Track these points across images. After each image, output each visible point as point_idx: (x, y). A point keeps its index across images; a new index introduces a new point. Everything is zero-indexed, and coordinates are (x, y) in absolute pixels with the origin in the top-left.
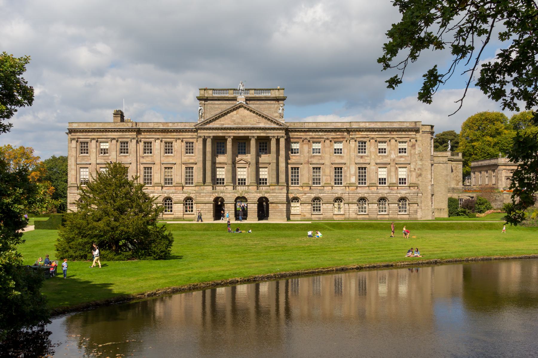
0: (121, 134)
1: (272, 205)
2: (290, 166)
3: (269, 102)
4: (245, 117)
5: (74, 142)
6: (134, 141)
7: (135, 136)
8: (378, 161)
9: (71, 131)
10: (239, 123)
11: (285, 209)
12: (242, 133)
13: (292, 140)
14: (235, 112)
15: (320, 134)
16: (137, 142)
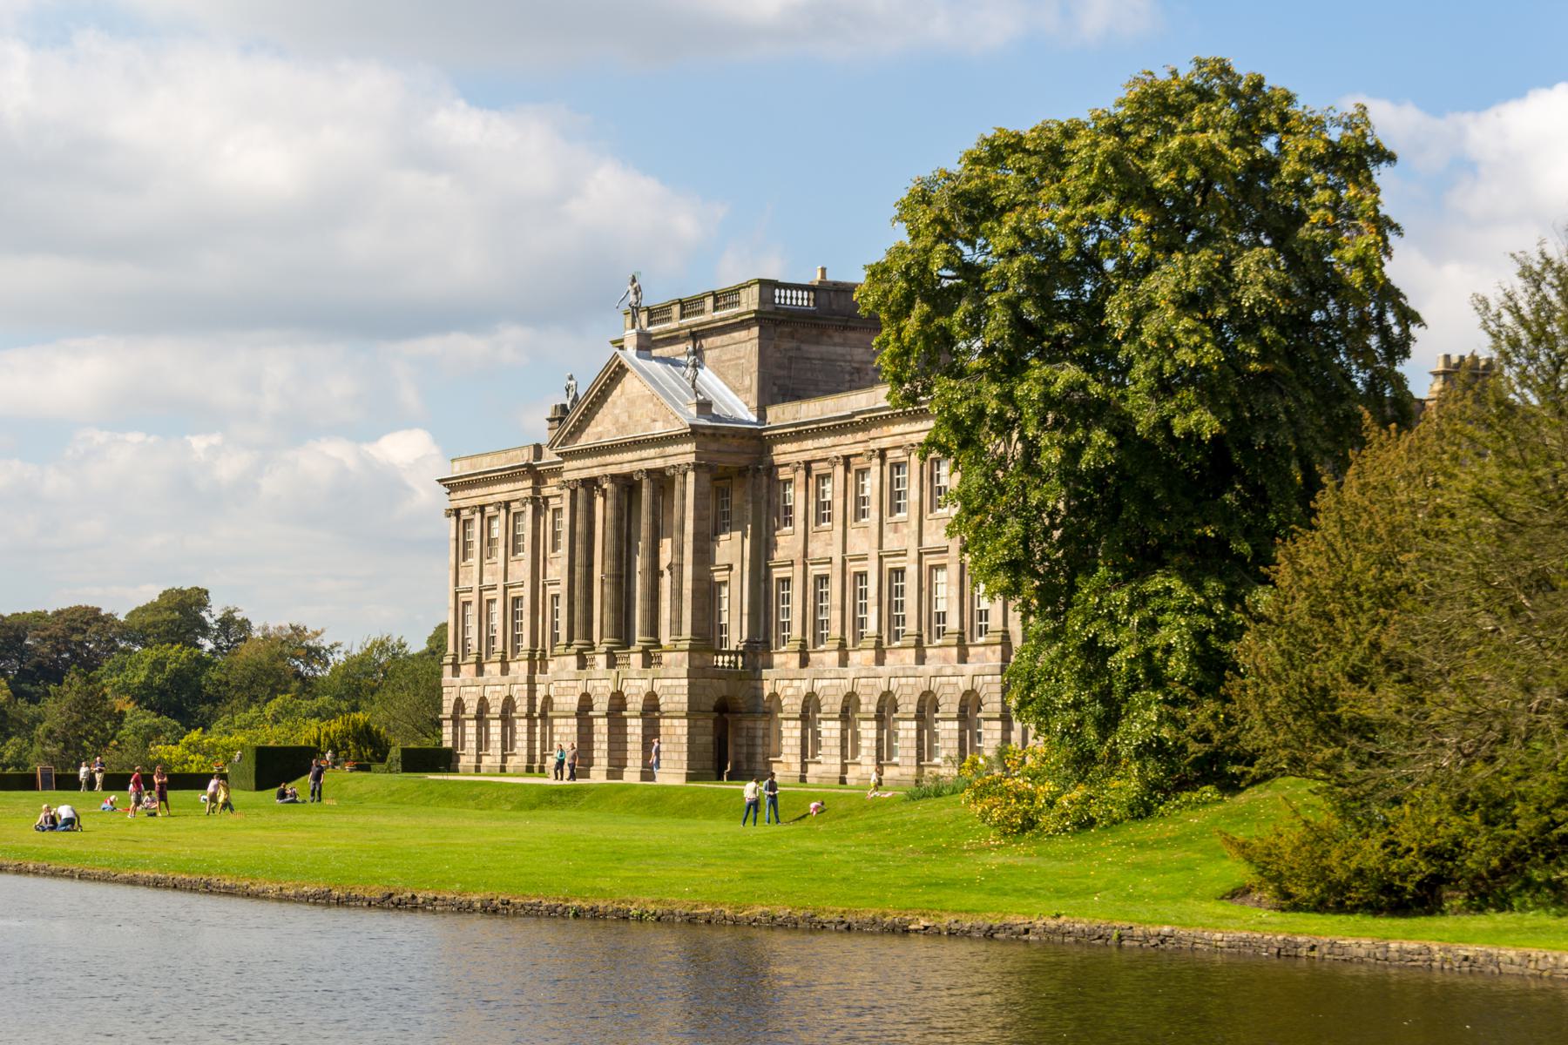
0: (511, 486)
1: (667, 722)
2: (777, 573)
3: (736, 335)
4: (632, 402)
5: (454, 519)
6: (529, 508)
7: (529, 493)
8: (928, 542)
9: (453, 485)
10: (624, 427)
11: (684, 740)
12: (626, 463)
13: (784, 474)
14: (619, 387)
15: (828, 441)
16: (537, 513)
